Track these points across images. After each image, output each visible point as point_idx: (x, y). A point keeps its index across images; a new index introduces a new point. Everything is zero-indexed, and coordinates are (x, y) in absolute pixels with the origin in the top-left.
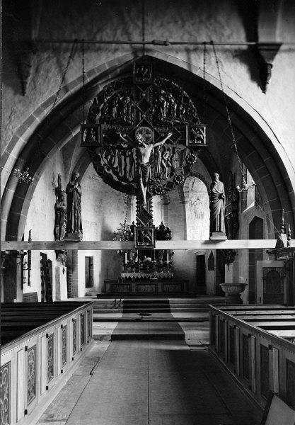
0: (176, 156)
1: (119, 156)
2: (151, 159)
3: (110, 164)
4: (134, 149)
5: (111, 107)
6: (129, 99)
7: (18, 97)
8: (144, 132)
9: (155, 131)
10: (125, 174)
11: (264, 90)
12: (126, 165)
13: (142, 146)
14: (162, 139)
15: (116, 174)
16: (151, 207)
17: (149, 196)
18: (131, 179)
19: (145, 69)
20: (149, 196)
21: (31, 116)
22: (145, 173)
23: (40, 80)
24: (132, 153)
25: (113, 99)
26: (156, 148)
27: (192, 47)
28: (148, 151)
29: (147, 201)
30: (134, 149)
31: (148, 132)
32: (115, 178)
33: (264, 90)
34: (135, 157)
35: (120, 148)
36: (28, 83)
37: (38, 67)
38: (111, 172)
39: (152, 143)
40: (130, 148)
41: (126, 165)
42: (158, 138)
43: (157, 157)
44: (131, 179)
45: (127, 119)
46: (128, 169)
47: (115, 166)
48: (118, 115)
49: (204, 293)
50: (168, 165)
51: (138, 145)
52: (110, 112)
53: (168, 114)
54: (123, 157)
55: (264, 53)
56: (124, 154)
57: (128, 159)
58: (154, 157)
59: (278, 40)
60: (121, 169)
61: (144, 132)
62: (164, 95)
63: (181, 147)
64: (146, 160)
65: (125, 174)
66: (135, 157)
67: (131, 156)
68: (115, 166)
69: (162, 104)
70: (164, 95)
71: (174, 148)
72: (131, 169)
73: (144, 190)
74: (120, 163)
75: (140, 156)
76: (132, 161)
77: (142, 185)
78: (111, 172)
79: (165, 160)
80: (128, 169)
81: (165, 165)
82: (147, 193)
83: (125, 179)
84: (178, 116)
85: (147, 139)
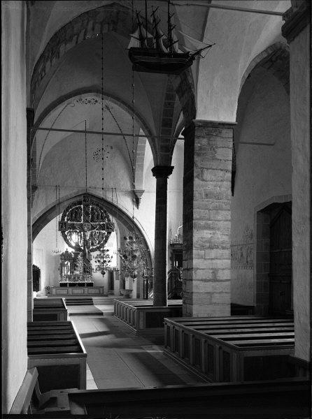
3: (71, 239)
14: (94, 228)
22: (87, 244)
23: (40, 201)
28: (88, 234)
40: (80, 232)
42: (93, 228)
49: (113, 294)
51: (84, 231)
52: (72, 217)
58: (91, 235)
59: (143, 189)
63: (104, 231)
67: (81, 235)
73: (87, 250)
75: (85, 236)
76: (81, 237)
85: (88, 228)
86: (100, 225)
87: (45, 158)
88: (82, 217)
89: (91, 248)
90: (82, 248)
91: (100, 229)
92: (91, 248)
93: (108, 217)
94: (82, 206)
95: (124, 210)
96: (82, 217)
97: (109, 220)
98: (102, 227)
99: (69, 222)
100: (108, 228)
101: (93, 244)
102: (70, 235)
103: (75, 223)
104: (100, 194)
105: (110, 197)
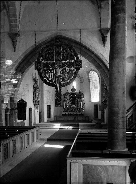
0: (71, 72)
1: (49, 72)
2: (61, 74)
3: (46, 76)
4: (54, 70)
5: (46, 55)
6: (52, 51)
7: (13, 52)
8: (58, 63)
9: (62, 63)
10: (51, 79)
11: (104, 46)
12: (51, 76)
13: (57, 69)
15: (48, 79)
16: (61, 92)
17: (60, 88)
18: (53, 81)
19: (58, 40)
20: (60, 88)
21: (17, 59)
24: (54, 71)
25: (47, 51)
26: (62, 69)
27: (76, 31)
28: (59, 71)
29: (59, 89)
30: (54, 70)
31: (59, 63)
32: (48, 81)
33: (104, 46)
34: (55, 73)
35: (49, 70)
36: (16, 47)
37: (20, 41)
38: (46, 79)
39: (61, 68)
40: (53, 70)
41: (51, 76)
42: (63, 65)
43: (63, 73)
44: (53, 81)
45: (52, 59)
46: (52, 77)
47: (47, 76)
48: (48, 57)
50: (67, 76)
52: (46, 57)
53: (67, 56)
54: (50, 73)
55: (103, 32)
56: (51, 72)
57: (52, 74)
58: (62, 72)
60: (50, 78)
61: (58, 63)
62: (66, 49)
63: (73, 68)
64: (59, 74)
65: (51, 79)
66: (55, 73)
68: (47, 76)
69: (65, 53)
70: (66, 49)
71: (70, 69)
72: (53, 78)
73: (58, 86)
74: (49, 75)
76: (54, 74)
77: (57, 84)
78: (46, 79)
79: (66, 74)
80: (52, 77)
81: (66, 76)
82: (59, 86)
83: (51, 81)
84: (71, 57)
85: (59, 66)
86: (69, 62)
87: (25, 9)
88: (54, 57)
89: (62, 83)
90: (55, 84)
91: (69, 66)
92: (62, 83)
93: (76, 56)
94: (54, 47)
95: (91, 48)
96: (54, 57)
97: (78, 58)
98: (71, 65)
99: (44, 62)
100: (76, 65)
101: (63, 80)
102: (45, 73)
103: (48, 62)
104: (70, 35)
105: (77, 37)
